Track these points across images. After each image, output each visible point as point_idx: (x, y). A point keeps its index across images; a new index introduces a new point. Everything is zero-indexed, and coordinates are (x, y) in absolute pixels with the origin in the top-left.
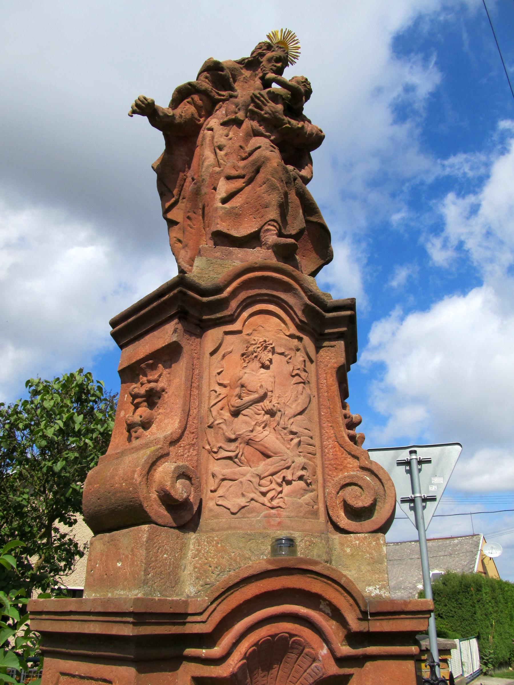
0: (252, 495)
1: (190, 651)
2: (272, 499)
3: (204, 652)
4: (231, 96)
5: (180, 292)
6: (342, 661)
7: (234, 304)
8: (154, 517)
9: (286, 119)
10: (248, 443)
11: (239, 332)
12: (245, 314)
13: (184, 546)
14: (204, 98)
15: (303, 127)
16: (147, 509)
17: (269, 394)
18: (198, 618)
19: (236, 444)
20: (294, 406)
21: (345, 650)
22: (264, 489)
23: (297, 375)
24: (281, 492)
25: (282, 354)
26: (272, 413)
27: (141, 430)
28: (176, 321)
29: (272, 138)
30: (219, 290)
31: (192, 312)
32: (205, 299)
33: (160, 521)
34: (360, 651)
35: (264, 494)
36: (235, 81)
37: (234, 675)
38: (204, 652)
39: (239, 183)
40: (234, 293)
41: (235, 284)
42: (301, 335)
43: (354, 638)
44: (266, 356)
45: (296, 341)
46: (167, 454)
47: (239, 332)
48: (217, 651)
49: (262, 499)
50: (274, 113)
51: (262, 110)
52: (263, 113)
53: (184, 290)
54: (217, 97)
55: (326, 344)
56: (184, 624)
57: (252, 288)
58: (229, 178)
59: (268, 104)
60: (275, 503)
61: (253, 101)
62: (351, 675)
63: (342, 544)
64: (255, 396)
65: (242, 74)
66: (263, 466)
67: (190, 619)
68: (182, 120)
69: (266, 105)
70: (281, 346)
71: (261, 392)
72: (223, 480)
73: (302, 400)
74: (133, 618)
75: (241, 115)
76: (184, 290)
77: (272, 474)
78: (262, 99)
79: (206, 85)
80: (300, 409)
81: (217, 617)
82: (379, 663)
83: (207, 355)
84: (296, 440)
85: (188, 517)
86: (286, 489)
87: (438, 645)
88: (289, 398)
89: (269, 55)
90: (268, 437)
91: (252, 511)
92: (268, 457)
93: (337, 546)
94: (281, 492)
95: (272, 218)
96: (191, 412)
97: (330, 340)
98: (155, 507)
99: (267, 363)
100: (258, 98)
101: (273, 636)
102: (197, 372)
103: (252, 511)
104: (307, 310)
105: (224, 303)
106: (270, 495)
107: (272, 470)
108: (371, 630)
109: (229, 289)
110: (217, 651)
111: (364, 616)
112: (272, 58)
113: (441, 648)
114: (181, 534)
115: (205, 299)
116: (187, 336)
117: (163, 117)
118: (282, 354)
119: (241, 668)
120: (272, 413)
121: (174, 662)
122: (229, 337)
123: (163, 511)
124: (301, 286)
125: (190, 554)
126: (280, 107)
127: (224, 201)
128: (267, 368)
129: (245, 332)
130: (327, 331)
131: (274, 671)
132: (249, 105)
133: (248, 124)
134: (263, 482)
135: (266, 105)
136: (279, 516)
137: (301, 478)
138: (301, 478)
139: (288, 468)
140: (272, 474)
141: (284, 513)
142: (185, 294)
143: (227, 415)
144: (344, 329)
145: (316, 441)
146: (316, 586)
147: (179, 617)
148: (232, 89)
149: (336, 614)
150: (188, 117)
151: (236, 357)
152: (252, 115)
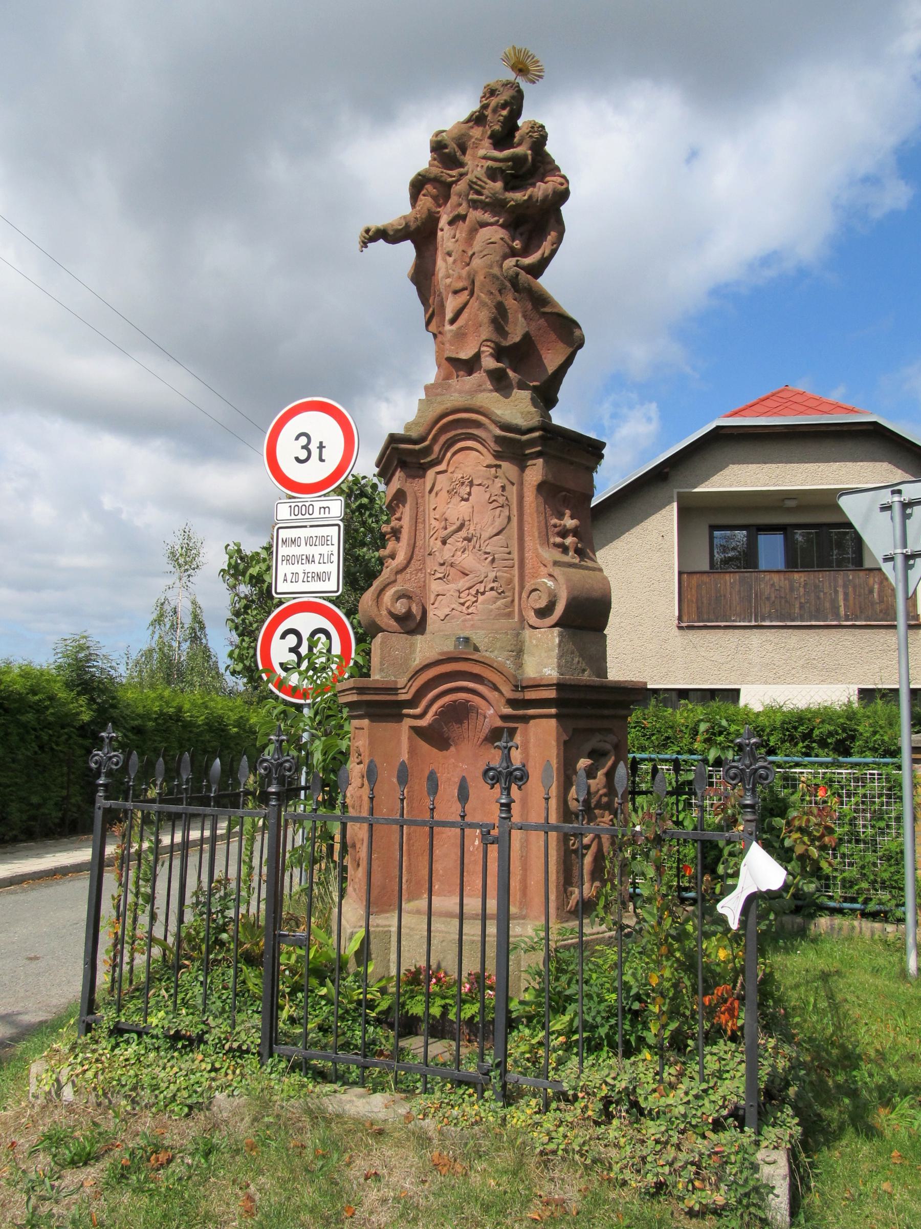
0: (453, 606)
1: (405, 711)
2: (468, 608)
3: (411, 711)
4: (462, 175)
5: (393, 448)
6: (504, 718)
7: (436, 448)
8: (383, 626)
9: (510, 195)
10: (452, 565)
11: (445, 471)
12: (449, 455)
13: (412, 646)
14: (438, 185)
15: (530, 197)
16: (379, 623)
17: (467, 523)
18: (404, 691)
19: (444, 567)
20: (490, 529)
21: (508, 711)
22: (462, 601)
23: (494, 501)
24: (476, 601)
25: (480, 485)
26: (469, 540)
27: (390, 560)
28: (399, 470)
29: (501, 221)
30: (423, 439)
31: (409, 459)
32: (417, 447)
33: (389, 630)
34: (521, 712)
35: (463, 604)
36: (464, 153)
37: (430, 725)
38: (411, 711)
39: (465, 296)
40: (435, 439)
41: (434, 432)
42: (498, 463)
43: (512, 703)
44: (465, 490)
45: (493, 470)
46: (395, 581)
47: (445, 471)
48: (418, 711)
49: (460, 608)
50: (494, 194)
51: (482, 195)
52: (483, 197)
53: (395, 445)
54: (450, 179)
55: (530, 463)
56: (397, 694)
57: (449, 431)
58: (456, 292)
59: (487, 186)
60: (470, 611)
61: (471, 188)
62: (516, 728)
63: (530, 637)
64: (454, 527)
65: (471, 137)
66: (463, 583)
67: (400, 691)
68: (419, 223)
69: (484, 188)
70: (479, 477)
71: (458, 524)
72: (438, 595)
73: (499, 523)
74: (556, 708)
75: (462, 210)
76: (395, 445)
77: (469, 589)
78: (479, 183)
79: (437, 171)
80: (495, 531)
81: (413, 690)
82: (537, 720)
83: (427, 493)
84: (490, 558)
85: (412, 625)
86: (481, 598)
87: (911, 741)
88: (486, 522)
89: (494, 102)
90: (468, 560)
91: (453, 617)
92: (467, 575)
93: (527, 639)
94: (476, 601)
95: (484, 338)
96: (417, 544)
97: (533, 459)
98: (386, 620)
99: (466, 496)
100: (475, 183)
101: (455, 701)
102: (421, 509)
103: (453, 617)
104: (498, 440)
105: (428, 451)
106: (467, 605)
107: (468, 585)
108: (526, 698)
109: (430, 437)
110: (418, 711)
111: (516, 688)
112: (497, 106)
113: (914, 745)
114: (409, 637)
115: (417, 447)
116: (410, 480)
117: (394, 235)
118: (480, 485)
119: (435, 720)
120: (469, 540)
121: (399, 718)
122: (439, 476)
123: (393, 623)
124: (490, 419)
125: (418, 650)
126: (499, 185)
127: (453, 321)
128: (467, 500)
129: (450, 470)
130: (528, 452)
131: (466, 725)
132: (468, 195)
133: (476, 215)
134: (462, 595)
135: (484, 188)
136: (472, 620)
137: (492, 589)
138: (492, 589)
139: (481, 582)
140: (469, 589)
141: (476, 618)
142: (397, 449)
143: (439, 543)
144: (539, 448)
145: (515, 555)
146: (476, 669)
147: (394, 690)
148: (462, 165)
149: (496, 688)
150: (424, 216)
151: (444, 494)
152: (474, 204)
